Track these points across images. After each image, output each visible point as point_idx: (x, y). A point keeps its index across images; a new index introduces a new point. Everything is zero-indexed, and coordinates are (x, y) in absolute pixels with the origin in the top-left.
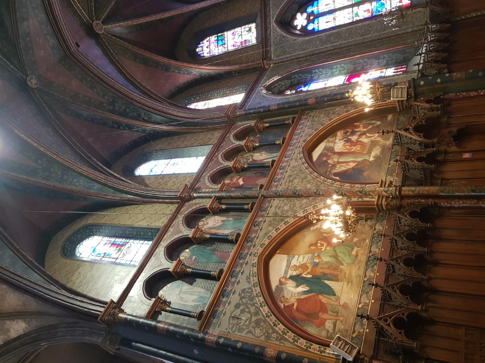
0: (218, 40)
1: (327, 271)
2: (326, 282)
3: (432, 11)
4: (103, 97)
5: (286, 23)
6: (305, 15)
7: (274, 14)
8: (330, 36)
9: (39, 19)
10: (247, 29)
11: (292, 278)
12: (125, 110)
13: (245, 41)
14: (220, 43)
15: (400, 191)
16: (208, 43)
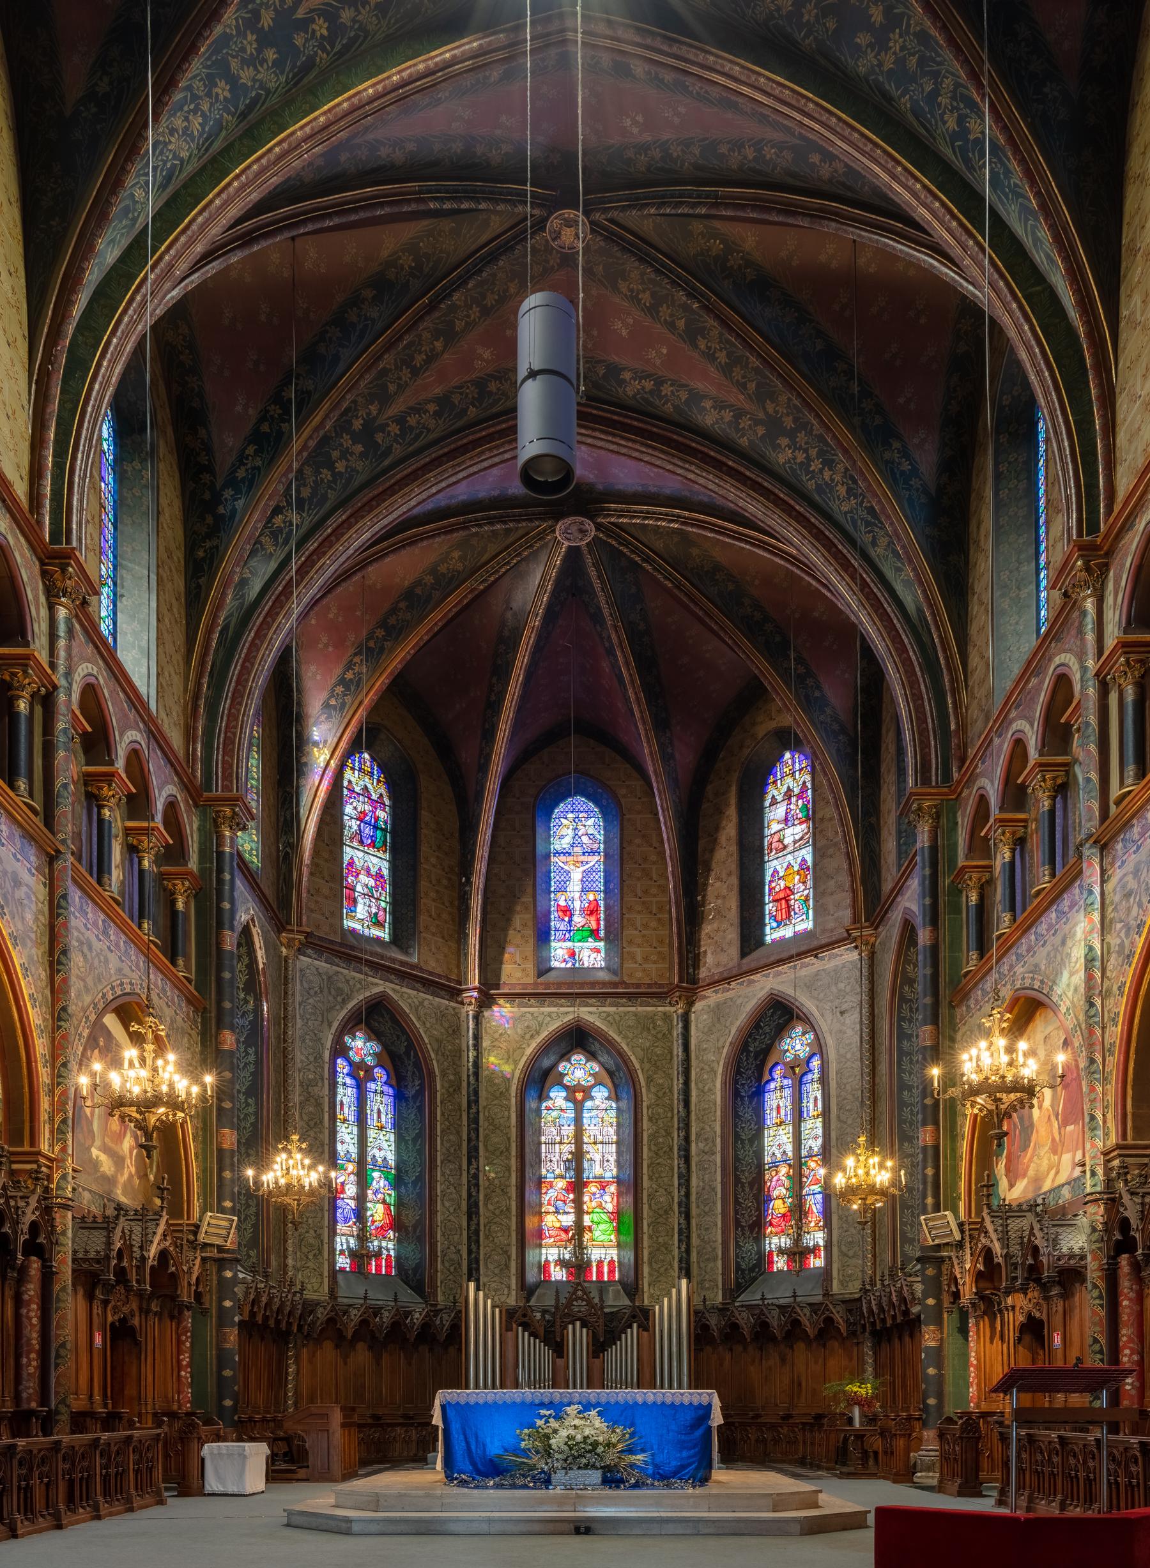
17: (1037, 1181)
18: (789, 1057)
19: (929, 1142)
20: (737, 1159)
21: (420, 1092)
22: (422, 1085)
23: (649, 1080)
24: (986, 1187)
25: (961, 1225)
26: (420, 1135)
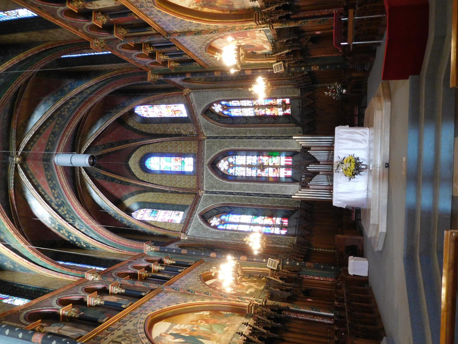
0: (152, 213)
1: (202, 335)
2: (200, 340)
4: (56, 198)
5: (206, 218)
6: (219, 220)
7: (200, 209)
9: (54, 130)
10: (177, 213)
11: (171, 334)
12: (65, 214)
13: (172, 220)
14: (153, 215)
15: (266, 302)
16: (144, 212)
17: (264, 42)
18: (221, 110)
19: (250, 71)
20: (253, 123)
22: (227, 207)
23: (227, 147)
24: (266, 55)
25: (277, 62)
26: (242, 208)
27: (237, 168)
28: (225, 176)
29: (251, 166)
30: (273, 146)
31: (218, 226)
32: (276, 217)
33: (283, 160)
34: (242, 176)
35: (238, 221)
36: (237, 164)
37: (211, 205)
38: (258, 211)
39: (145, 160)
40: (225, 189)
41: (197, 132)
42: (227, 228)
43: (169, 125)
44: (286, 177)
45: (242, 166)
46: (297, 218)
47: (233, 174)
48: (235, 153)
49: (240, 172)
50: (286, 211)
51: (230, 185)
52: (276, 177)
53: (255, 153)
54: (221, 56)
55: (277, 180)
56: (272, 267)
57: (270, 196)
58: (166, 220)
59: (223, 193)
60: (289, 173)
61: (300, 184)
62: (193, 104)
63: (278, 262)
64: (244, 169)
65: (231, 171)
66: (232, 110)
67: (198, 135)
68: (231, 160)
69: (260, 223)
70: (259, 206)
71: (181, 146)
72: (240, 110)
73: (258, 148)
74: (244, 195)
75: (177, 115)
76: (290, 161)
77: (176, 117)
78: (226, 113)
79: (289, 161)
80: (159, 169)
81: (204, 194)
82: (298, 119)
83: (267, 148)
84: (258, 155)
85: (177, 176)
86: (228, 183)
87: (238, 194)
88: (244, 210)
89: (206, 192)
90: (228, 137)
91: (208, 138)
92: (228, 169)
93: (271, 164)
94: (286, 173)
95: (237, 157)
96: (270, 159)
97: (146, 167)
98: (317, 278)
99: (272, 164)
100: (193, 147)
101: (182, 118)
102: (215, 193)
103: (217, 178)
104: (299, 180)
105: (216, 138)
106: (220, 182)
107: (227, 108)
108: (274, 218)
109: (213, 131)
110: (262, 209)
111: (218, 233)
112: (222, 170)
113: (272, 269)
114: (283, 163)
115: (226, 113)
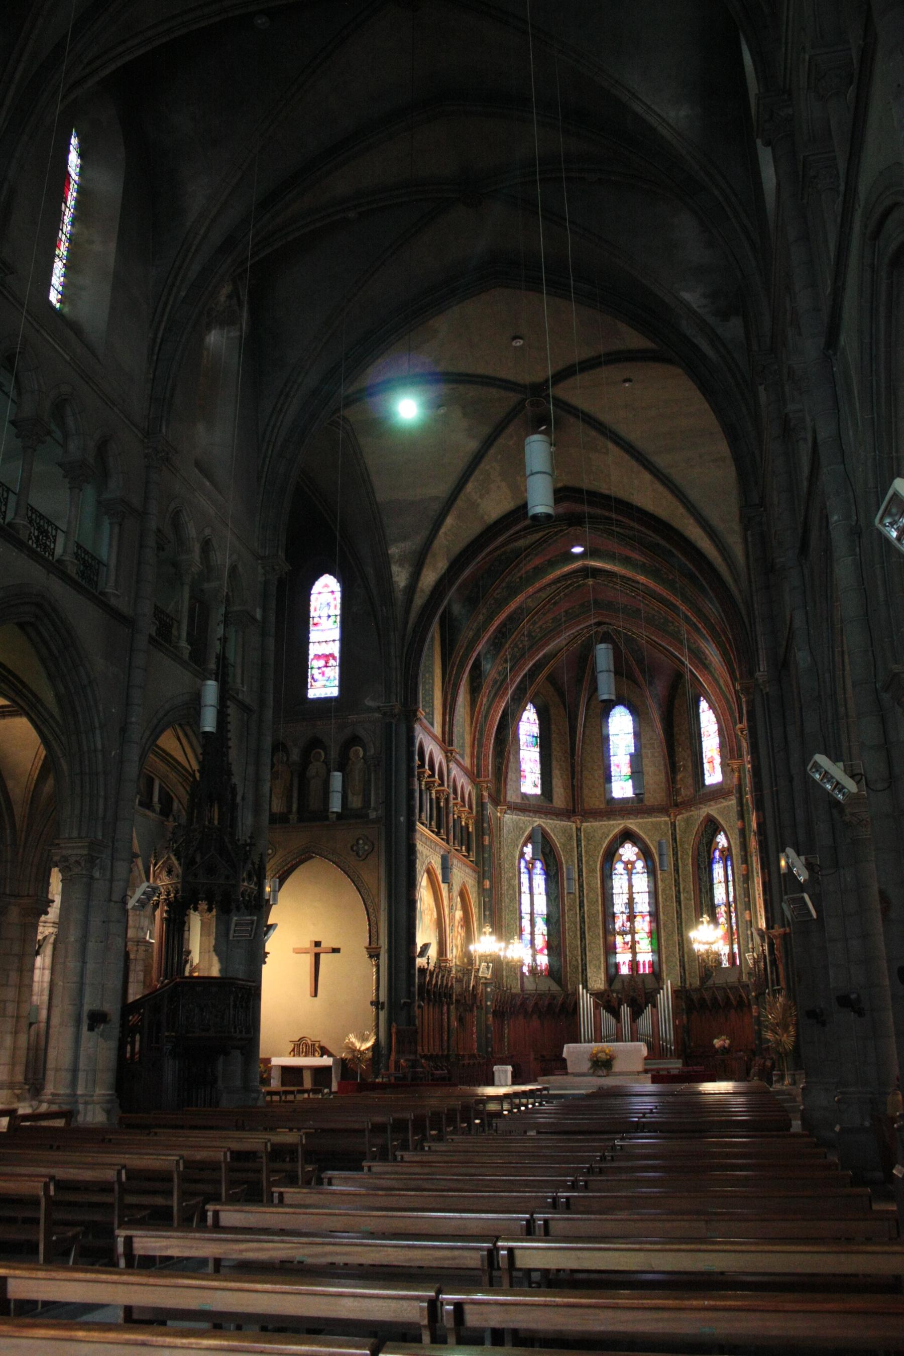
3: (516, 995)
4: (541, 627)
7: (550, 824)
8: (514, 889)
14: (530, 739)
16: (532, 721)
21: (557, 873)
26: (557, 897)
27: (626, 877)
28: (611, 856)
29: (631, 903)
30: (667, 940)
31: (524, 859)
32: (549, 955)
33: (645, 956)
34: (612, 888)
35: (536, 891)
36: (634, 877)
37: (557, 840)
38: (556, 923)
39: (625, 706)
40: (587, 862)
41: (681, 803)
42: (522, 875)
43: (689, 751)
44: (617, 966)
45: (631, 886)
46: (549, 990)
47: (616, 872)
48: (651, 871)
49: (619, 883)
50: (559, 970)
51: (594, 870)
52: (615, 948)
53: (654, 910)
54: (705, 923)
55: (610, 950)
56: (481, 970)
57: (581, 941)
58: (523, 767)
59: (580, 860)
60: (625, 970)
61: (605, 990)
62: (722, 800)
63: (489, 977)
64: (626, 890)
65: (619, 867)
66: (721, 865)
67: (676, 805)
68: (640, 865)
69: (536, 929)
70: (564, 926)
71: (655, 775)
72: (723, 880)
73: (661, 914)
74: (580, 897)
75: (706, 766)
76: (645, 970)
77: (702, 764)
78: (717, 854)
79: (644, 967)
80: (611, 733)
81: (574, 826)
82: (710, 983)
83: (662, 931)
84: (650, 914)
85: (601, 772)
86: (598, 866)
87: (581, 886)
88: (555, 900)
89: (578, 830)
90: (677, 860)
91: (673, 825)
92: (623, 862)
93: (637, 937)
94: (624, 963)
95: (646, 875)
96: (645, 936)
97: (614, 707)
98: (475, 1029)
99: (637, 939)
100: (655, 796)
101: (703, 774)
102: (579, 845)
103: (604, 846)
104: (612, 988)
105: (674, 839)
106: (599, 852)
107: (726, 855)
108: (546, 952)
109: (685, 832)
110: (559, 931)
111: (513, 865)
112: (621, 851)
113: (478, 970)
114: (640, 958)
115: (717, 854)
